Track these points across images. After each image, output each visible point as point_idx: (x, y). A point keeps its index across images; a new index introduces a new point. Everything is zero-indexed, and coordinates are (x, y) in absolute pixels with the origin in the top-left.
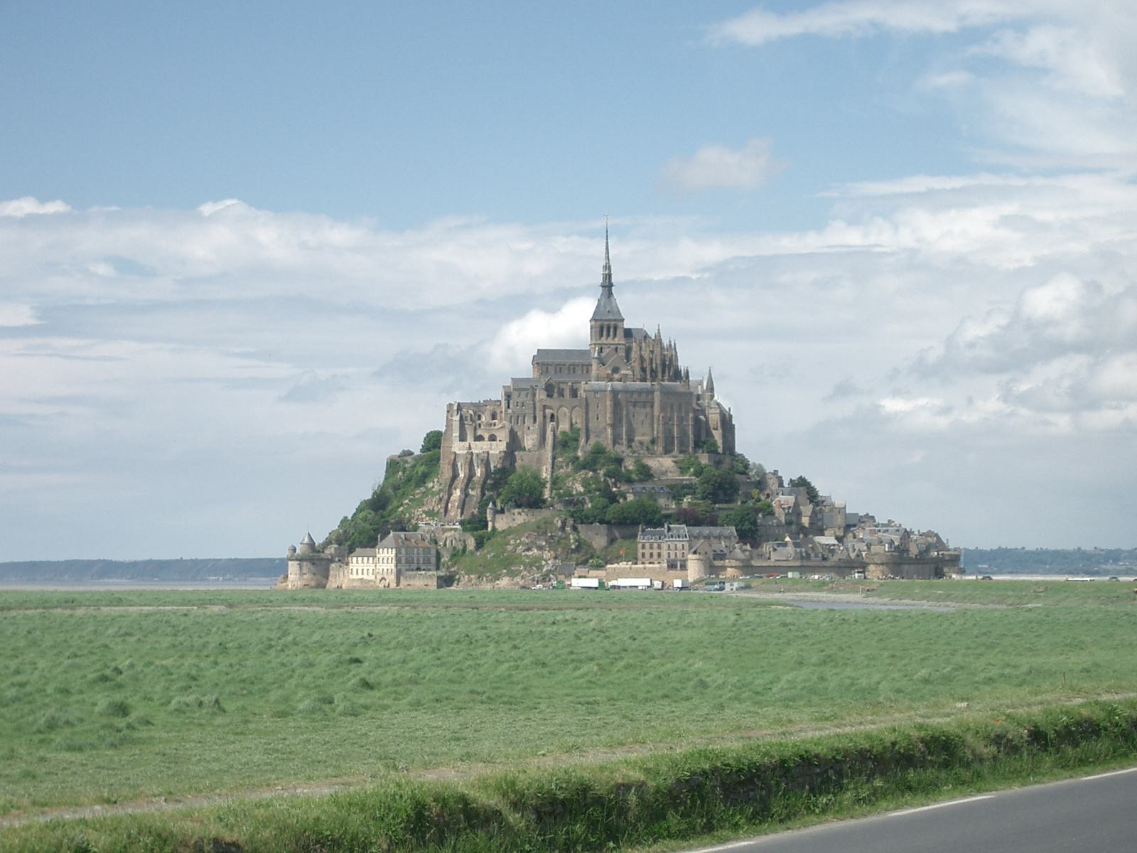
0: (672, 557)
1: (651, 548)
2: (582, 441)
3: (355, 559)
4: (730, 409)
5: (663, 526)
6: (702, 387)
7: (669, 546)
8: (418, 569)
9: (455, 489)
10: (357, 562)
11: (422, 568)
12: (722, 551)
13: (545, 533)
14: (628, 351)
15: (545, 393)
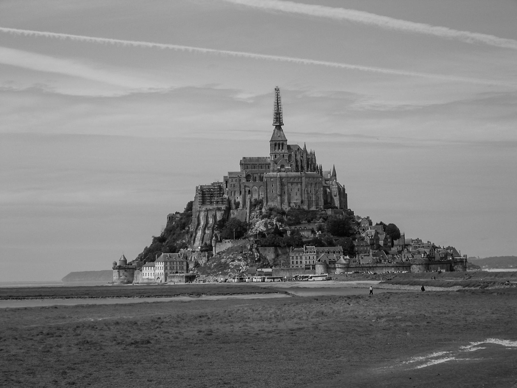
0: (308, 263)
1: (297, 259)
2: (265, 203)
3: (145, 268)
4: (344, 186)
5: (303, 247)
6: (330, 175)
7: (306, 258)
8: (177, 273)
9: (199, 230)
10: (146, 270)
11: (179, 272)
12: (334, 259)
13: (242, 252)
14: (290, 156)
15: (245, 179)
